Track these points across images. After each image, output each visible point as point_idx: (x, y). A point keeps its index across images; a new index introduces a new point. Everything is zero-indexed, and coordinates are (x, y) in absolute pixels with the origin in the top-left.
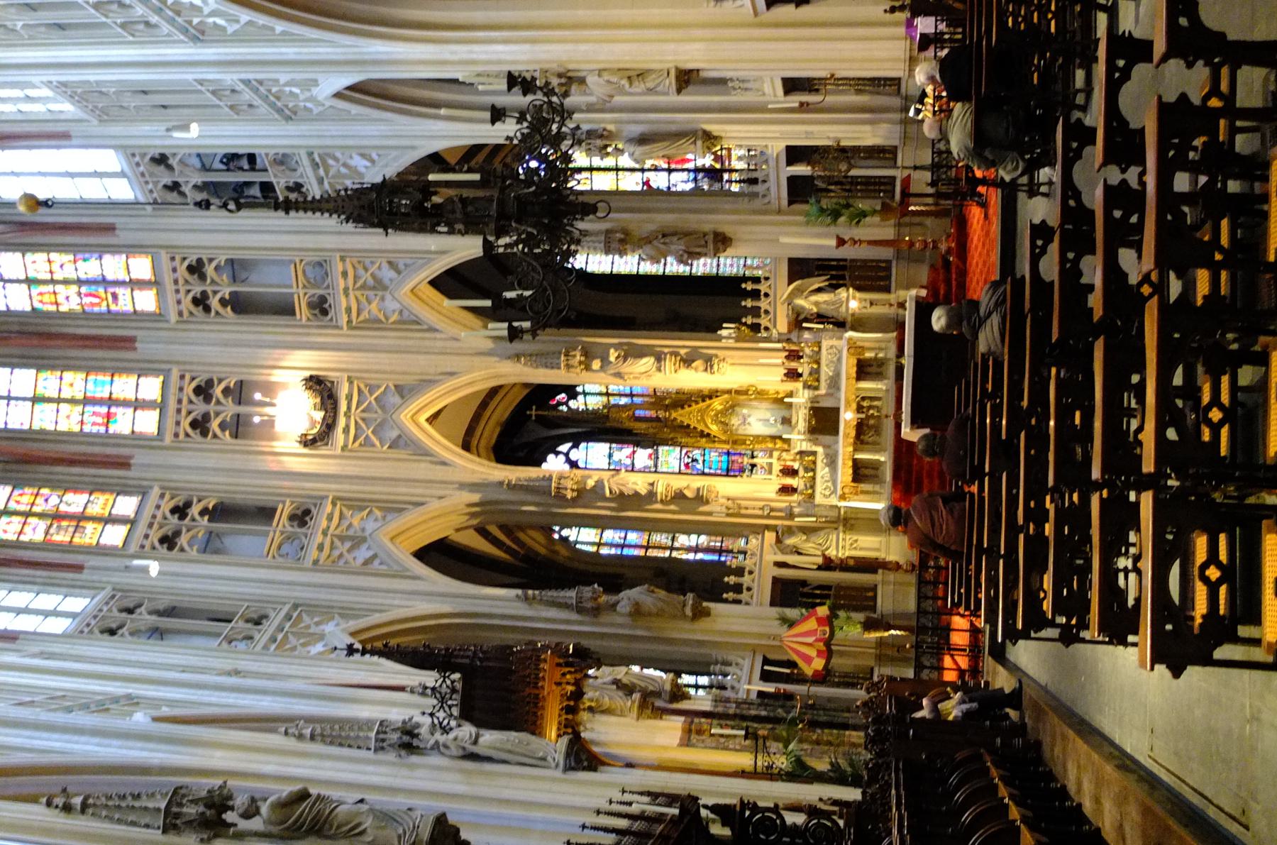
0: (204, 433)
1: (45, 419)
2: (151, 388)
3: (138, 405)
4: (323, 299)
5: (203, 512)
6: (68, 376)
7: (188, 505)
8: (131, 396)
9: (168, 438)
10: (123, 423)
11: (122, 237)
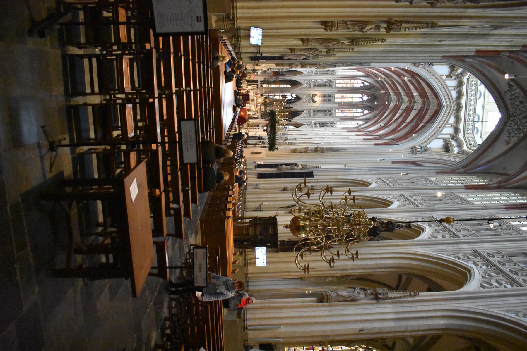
0: (329, 95)
1: (351, 95)
2: (336, 100)
3: (338, 98)
4: (314, 112)
5: (327, 85)
6: (348, 101)
7: (329, 86)
8: (339, 99)
9: (333, 94)
10: (340, 96)
11: (339, 118)
